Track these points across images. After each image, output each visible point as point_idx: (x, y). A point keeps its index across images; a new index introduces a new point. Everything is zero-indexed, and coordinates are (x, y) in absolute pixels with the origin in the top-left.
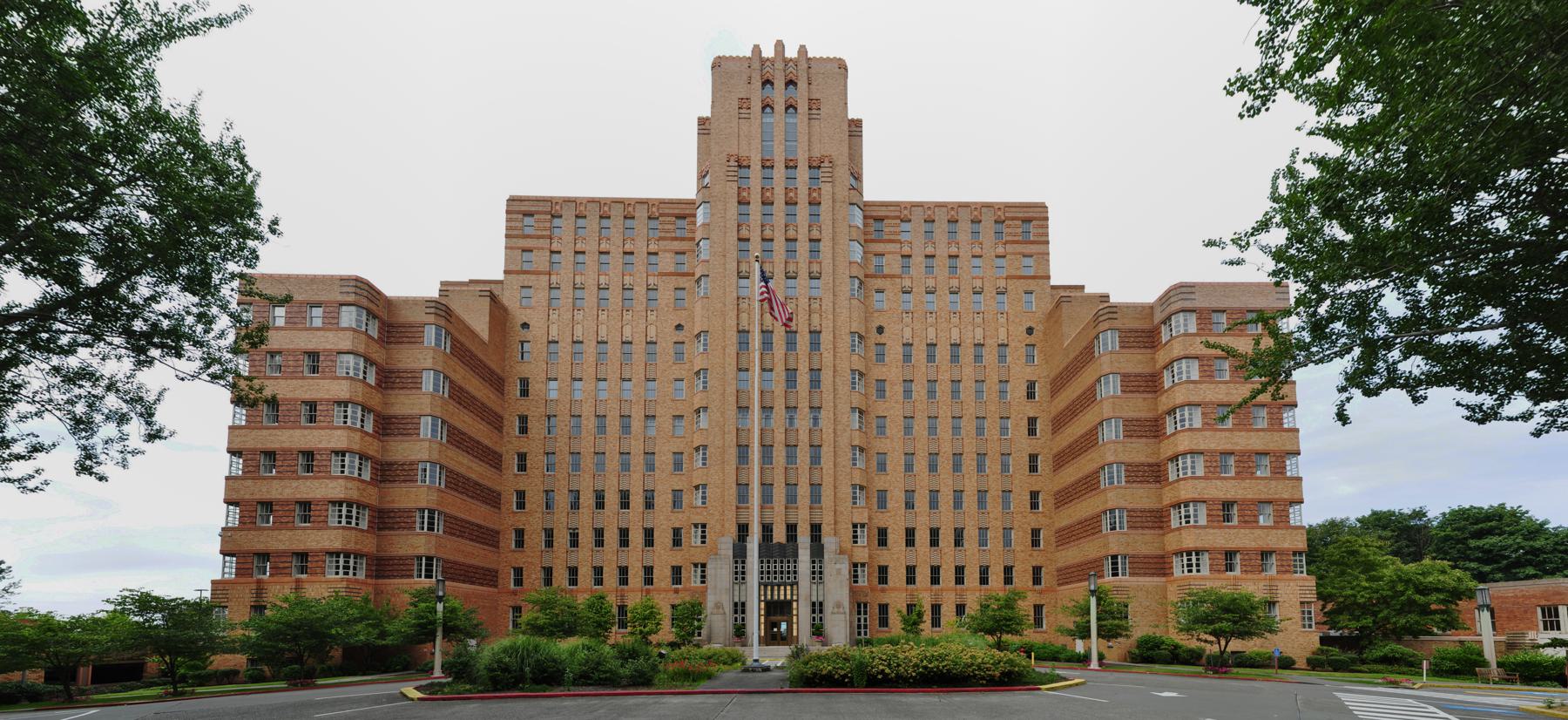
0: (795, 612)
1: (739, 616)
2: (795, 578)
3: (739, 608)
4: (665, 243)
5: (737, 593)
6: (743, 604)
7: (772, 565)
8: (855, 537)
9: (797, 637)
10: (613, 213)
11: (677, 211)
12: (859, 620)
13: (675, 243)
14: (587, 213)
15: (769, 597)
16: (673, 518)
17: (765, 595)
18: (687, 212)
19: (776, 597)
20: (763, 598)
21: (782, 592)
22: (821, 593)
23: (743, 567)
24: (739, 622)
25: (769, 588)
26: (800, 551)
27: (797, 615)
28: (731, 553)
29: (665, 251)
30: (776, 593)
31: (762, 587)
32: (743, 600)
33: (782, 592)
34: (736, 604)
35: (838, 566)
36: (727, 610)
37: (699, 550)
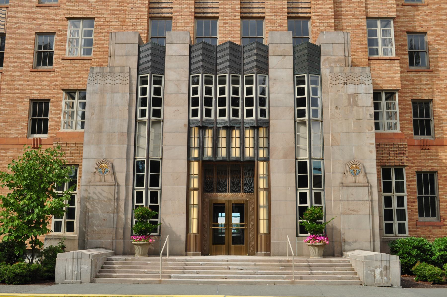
0: (262, 184)
2: (263, 113)
3: (146, 174)
5: (143, 143)
8: (372, 42)
9: (268, 235)
12: (388, 201)
15: (209, 152)
16: (40, 17)
17: (201, 148)
19: (223, 153)
20: (195, 153)
21: (236, 142)
22: (316, 142)
23: (157, 91)
24: (146, 202)
25: (209, 133)
26: (273, 61)
27: (268, 190)
28: (133, 62)
30: (223, 143)
31: (195, 132)
33: (236, 142)
35: (351, 89)
36: (121, 178)
37: (77, 65)
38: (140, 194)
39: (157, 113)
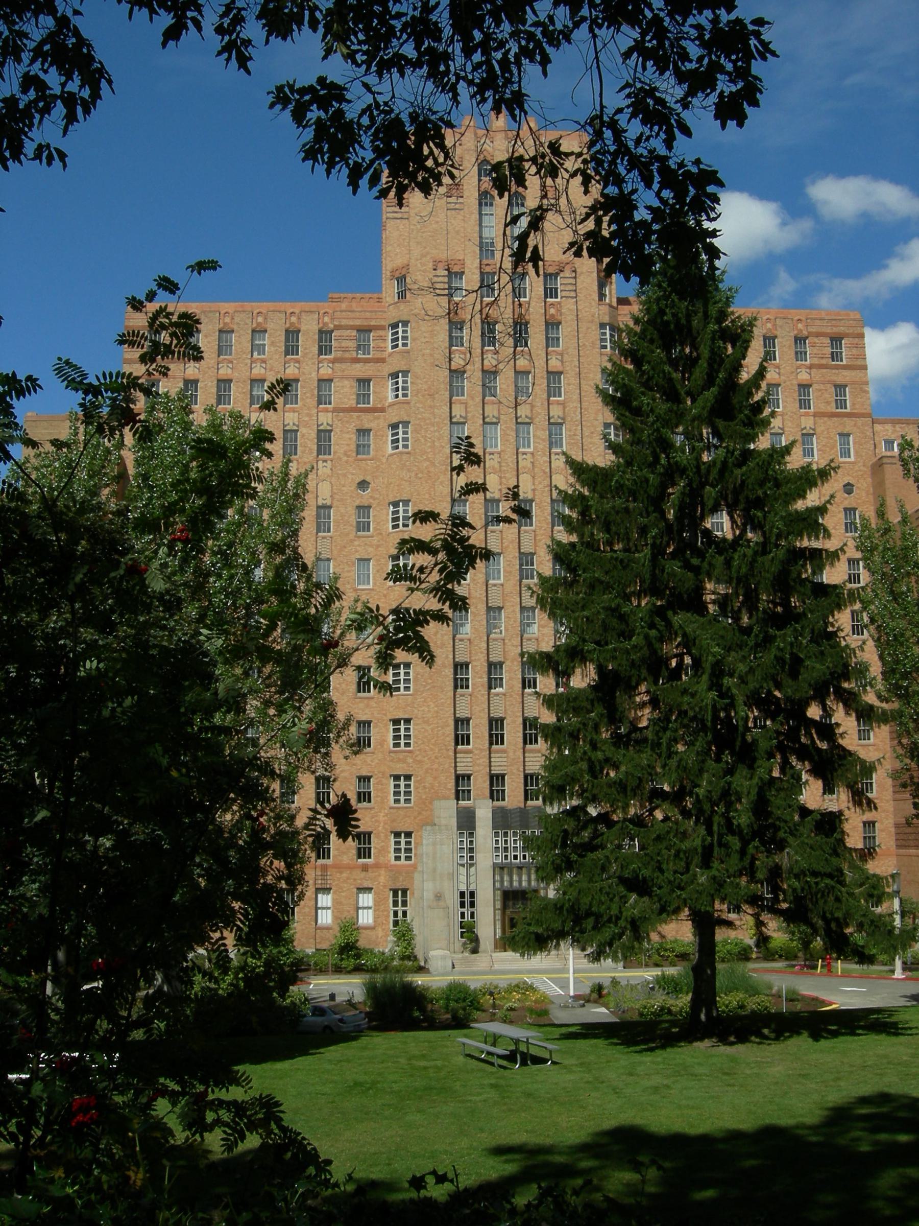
1: (467, 911)
3: (467, 900)
4: (343, 366)
6: (472, 894)
7: (511, 839)
10: (270, 326)
11: (358, 323)
13: (358, 366)
14: (235, 327)
17: (502, 881)
18: (373, 323)
19: (515, 884)
20: (498, 885)
21: (524, 877)
29: (342, 378)
32: (472, 888)
34: (462, 894)
36: (450, 903)
37: (401, 812)
38: (463, 915)
39: (472, 858)
